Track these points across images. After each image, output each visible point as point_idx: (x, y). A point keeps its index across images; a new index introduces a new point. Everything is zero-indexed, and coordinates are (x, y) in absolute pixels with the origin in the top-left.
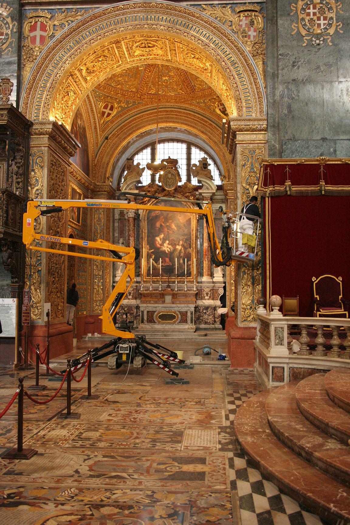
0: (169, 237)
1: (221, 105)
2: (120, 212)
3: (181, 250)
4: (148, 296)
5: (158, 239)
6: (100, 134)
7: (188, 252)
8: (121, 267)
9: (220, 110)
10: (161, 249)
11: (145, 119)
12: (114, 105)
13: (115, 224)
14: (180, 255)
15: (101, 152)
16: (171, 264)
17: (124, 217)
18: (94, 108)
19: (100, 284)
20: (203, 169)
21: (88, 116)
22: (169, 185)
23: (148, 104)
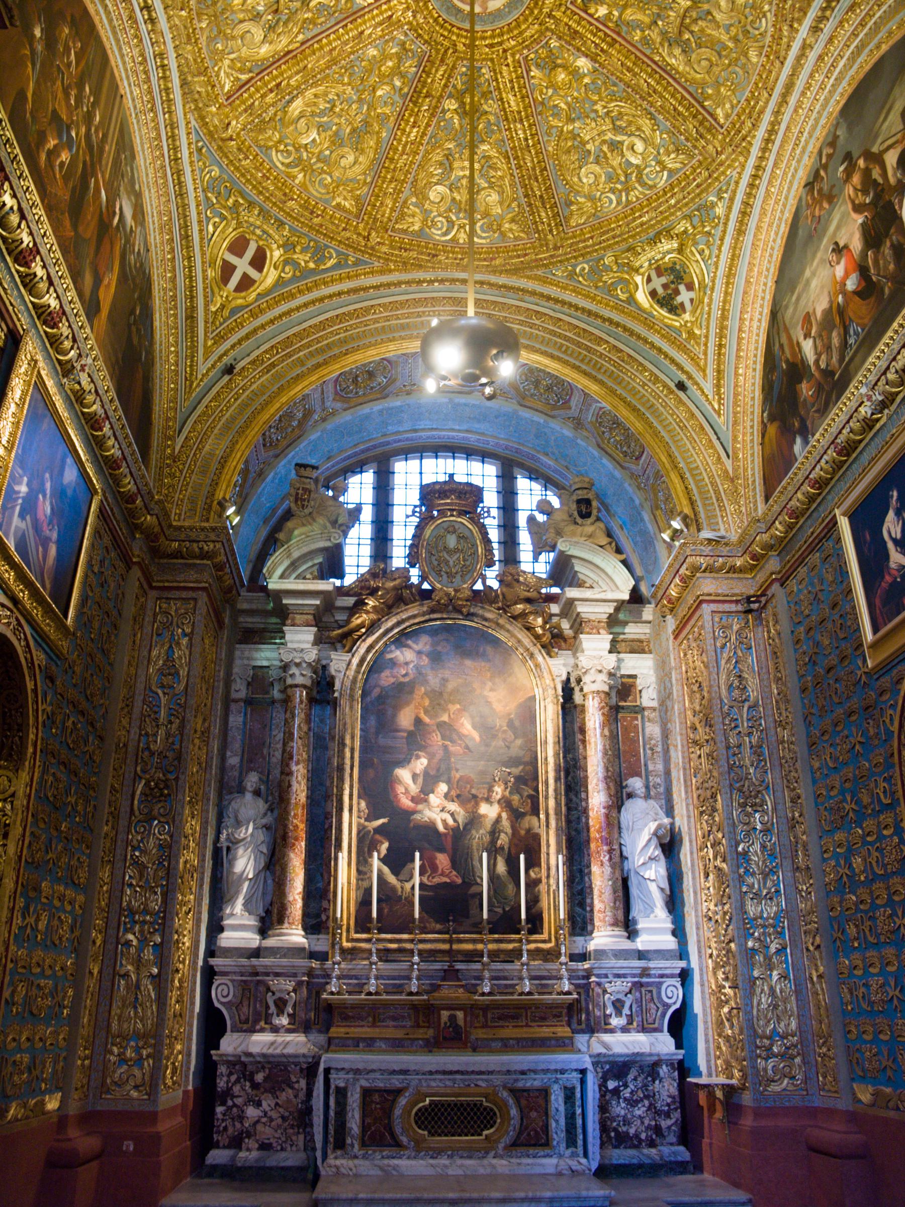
0: (449, 769)
1: (659, 275)
2: (254, 677)
3: (498, 820)
4: (361, 1018)
5: (404, 774)
6: (205, 346)
7: (528, 831)
8: (246, 885)
9: (653, 294)
10: (417, 817)
11: (376, 321)
12: (272, 251)
13: (231, 719)
14: (494, 841)
15: (204, 413)
16: (459, 881)
17: (267, 693)
18: (196, 228)
19: (148, 954)
20: (579, 520)
21: (167, 248)
22: (450, 575)
23: (390, 271)
